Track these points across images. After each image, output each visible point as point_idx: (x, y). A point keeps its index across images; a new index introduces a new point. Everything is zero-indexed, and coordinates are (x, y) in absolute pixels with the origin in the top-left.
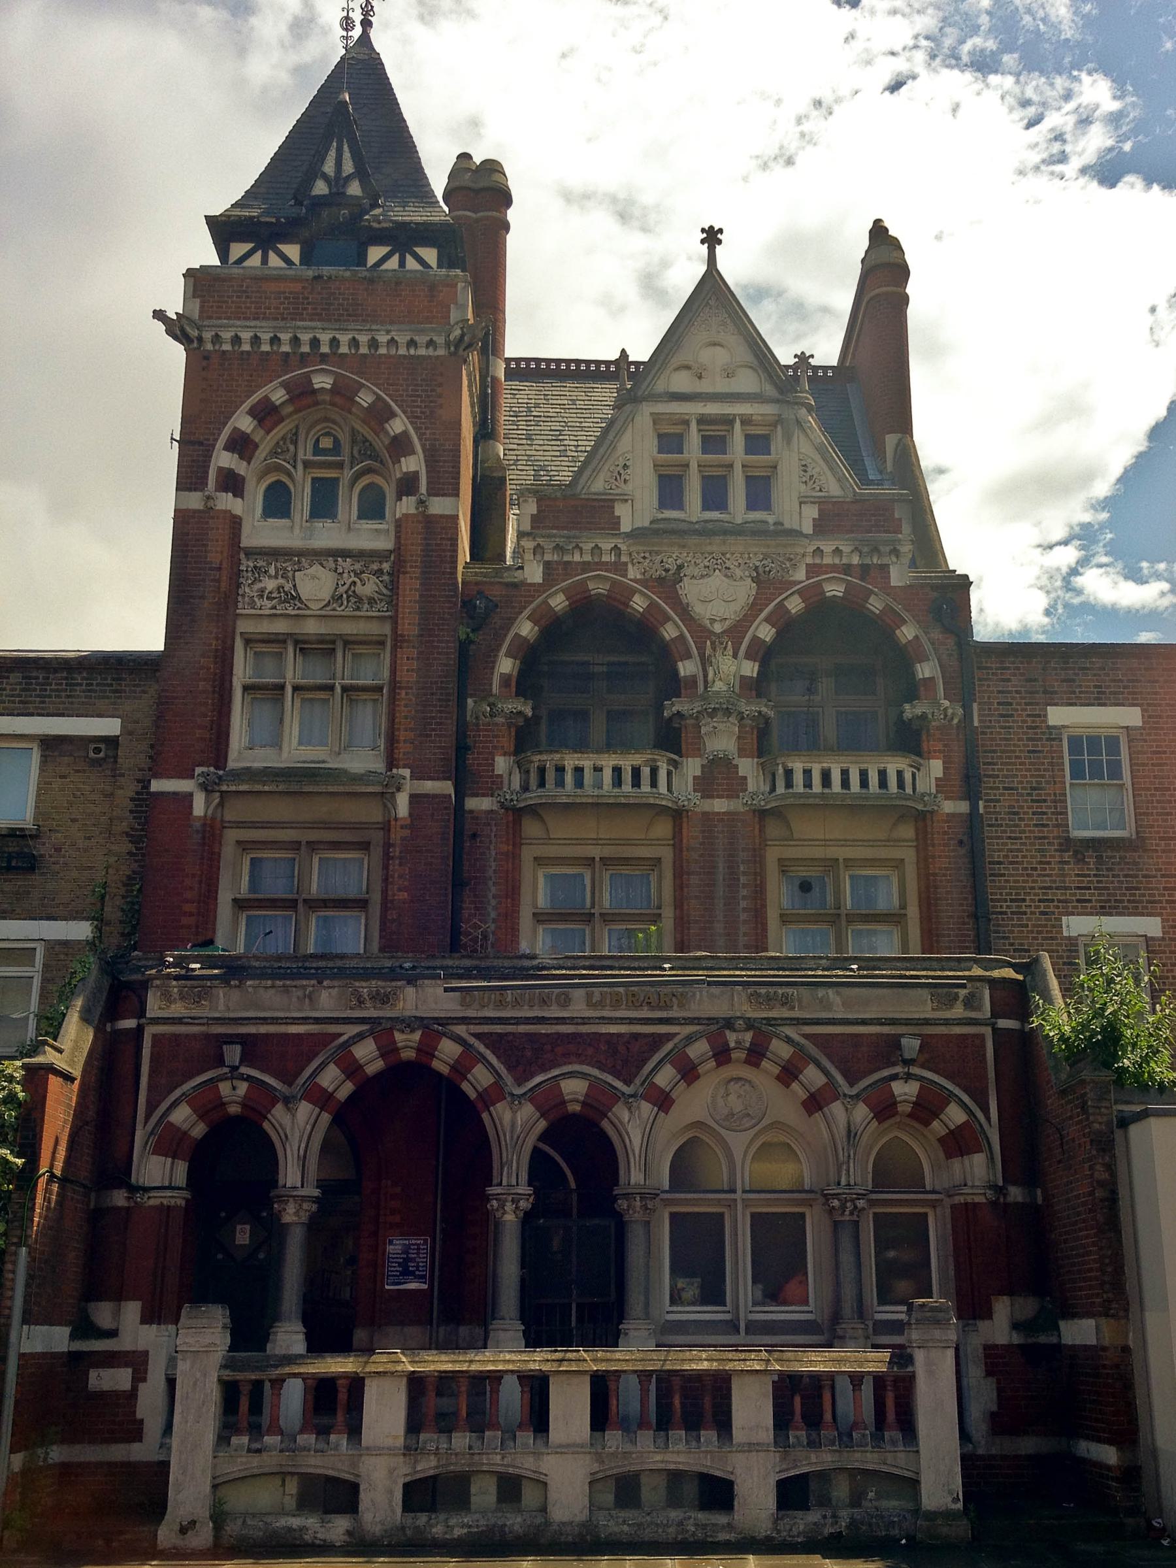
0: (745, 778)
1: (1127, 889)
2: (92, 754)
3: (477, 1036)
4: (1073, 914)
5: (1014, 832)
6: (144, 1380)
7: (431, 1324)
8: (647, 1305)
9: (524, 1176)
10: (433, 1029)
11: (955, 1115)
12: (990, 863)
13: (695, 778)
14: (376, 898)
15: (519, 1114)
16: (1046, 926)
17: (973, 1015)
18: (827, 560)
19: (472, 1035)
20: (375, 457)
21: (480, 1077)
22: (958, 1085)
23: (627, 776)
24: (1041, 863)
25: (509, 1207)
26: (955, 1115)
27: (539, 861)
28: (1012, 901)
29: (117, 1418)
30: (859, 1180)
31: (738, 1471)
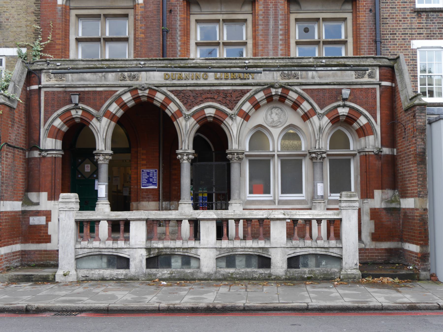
1: (438, 28)
3: (172, 91)
4: (415, 39)
5: (393, 5)
6: (50, 221)
7: (159, 200)
8: (239, 194)
9: (191, 146)
10: (153, 89)
11: (363, 121)
12: (382, 18)
15: (188, 123)
16: (404, 44)
19: (169, 91)
24: (403, 18)
25: (185, 157)
26: (363, 121)
27: (197, 21)
28: (391, 34)
29: (41, 234)
30: (323, 147)
31: (272, 255)
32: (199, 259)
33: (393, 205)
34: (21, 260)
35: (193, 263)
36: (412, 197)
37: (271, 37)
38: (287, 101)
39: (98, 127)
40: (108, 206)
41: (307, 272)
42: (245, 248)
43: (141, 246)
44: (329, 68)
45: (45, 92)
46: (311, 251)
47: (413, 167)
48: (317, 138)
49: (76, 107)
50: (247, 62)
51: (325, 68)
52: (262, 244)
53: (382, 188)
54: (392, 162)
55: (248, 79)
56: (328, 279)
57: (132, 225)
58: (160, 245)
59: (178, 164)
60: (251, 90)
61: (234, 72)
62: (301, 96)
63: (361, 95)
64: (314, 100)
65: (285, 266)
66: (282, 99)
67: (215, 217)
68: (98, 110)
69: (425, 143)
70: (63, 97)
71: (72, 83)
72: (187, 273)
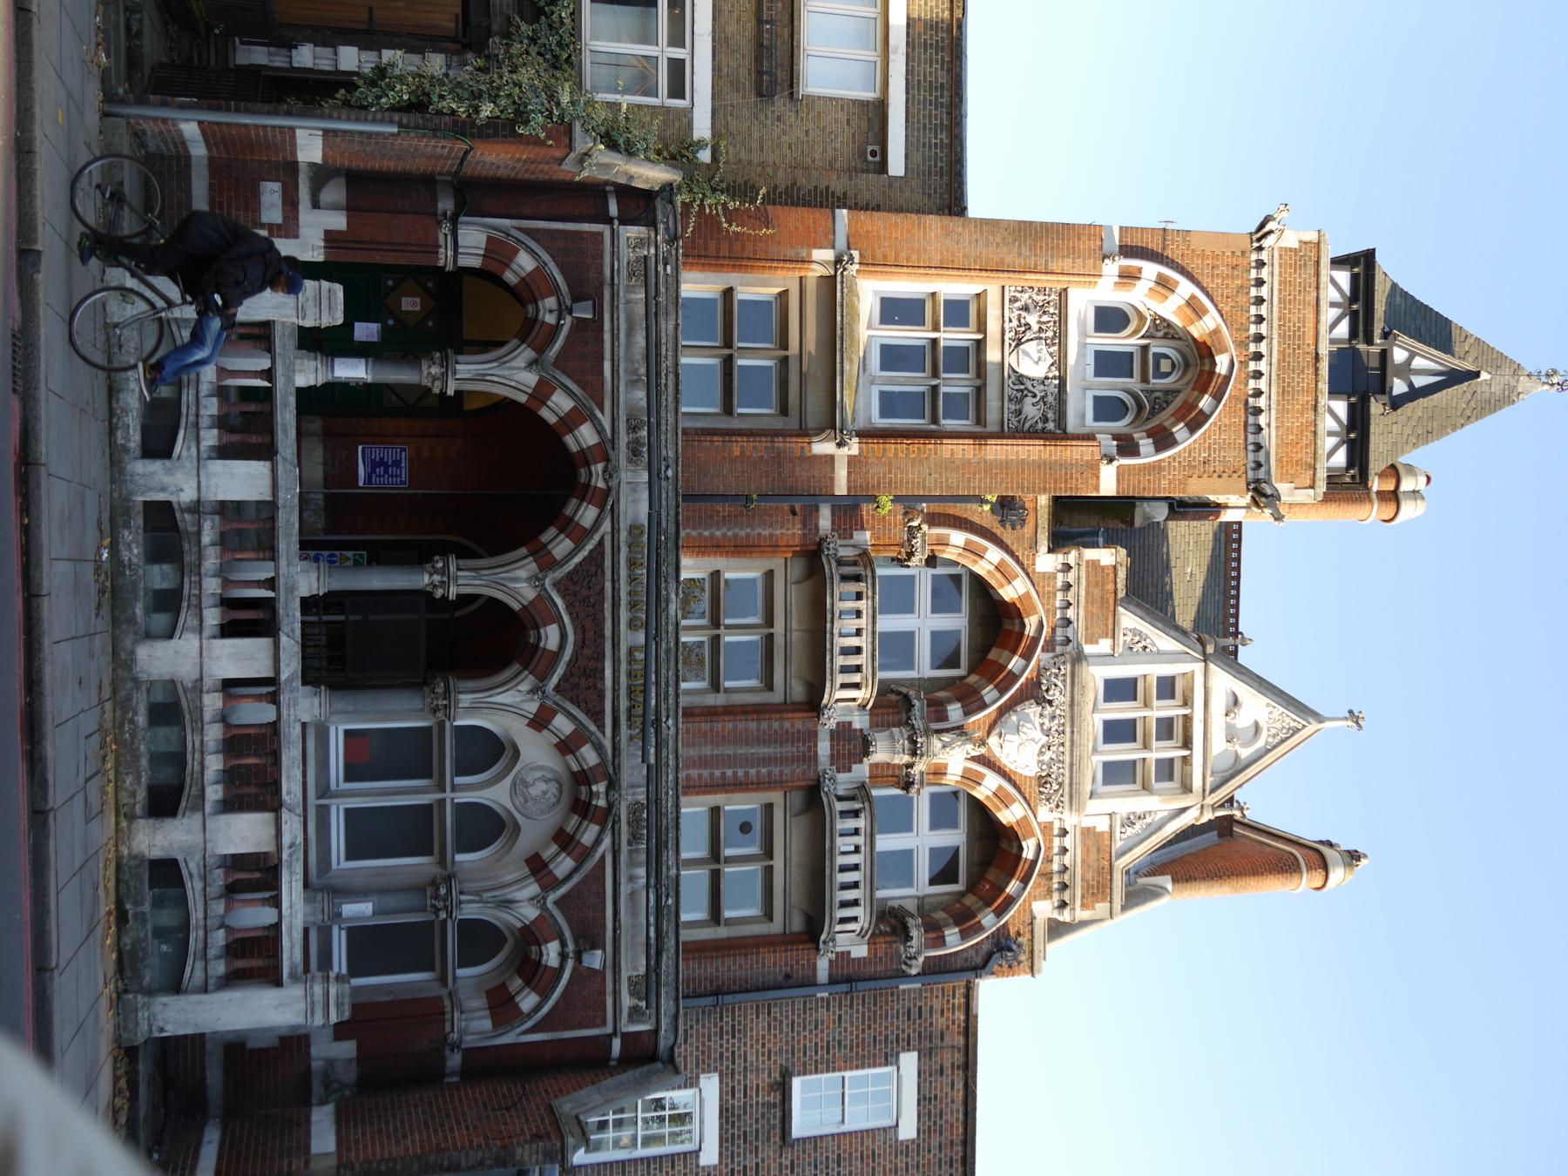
0: (850, 770)
2: (870, 148)
3: (601, 543)
10: (605, 499)
11: (528, 1001)
13: (850, 723)
14: (734, 424)
17: (625, 1014)
18: (1056, 842)
19: (602, 538)
20: (1153, 413)
21: (561, 547)
22: (557, 1003)
23: (853, 660)
25: (437, 578)
26: (528, 1001)
31: (185, 821)
32: (170, 636)
33: (317, 1089)
34: (162, 156)
35: (160, 620)
36: (339, 1143)
37: (729, 751)
38: (575, 819)
39: (514, 364)
40: (312, 383)
41: (139, 909)
42: (202, 753)
43: (203, 489)
44: (652, 919)
45: (601, 234)
46: (196, 915)
47: (413, 1141)
48: (486, 895)
49: (562, 311)
50: (670, 722)
51: (652, 910)
52: (214, 793)
53: (362, 1057)
54: (428, 1074)
55: (630, 727)
56: (126, 966)
57: (259, 468)
58: (206, 539)
59: (418, 556)
60: (604, 733)
61: (645, 692)
62: (587, 853)
63: (587, 995)
64: (578, 884)
65: (156, 853)
66: (582, 808)
67: (283, 677)
68: (558, 363)
69: (472, 1168)
70: (586, 283)
71: (622, 301)
72: (133, 607)
